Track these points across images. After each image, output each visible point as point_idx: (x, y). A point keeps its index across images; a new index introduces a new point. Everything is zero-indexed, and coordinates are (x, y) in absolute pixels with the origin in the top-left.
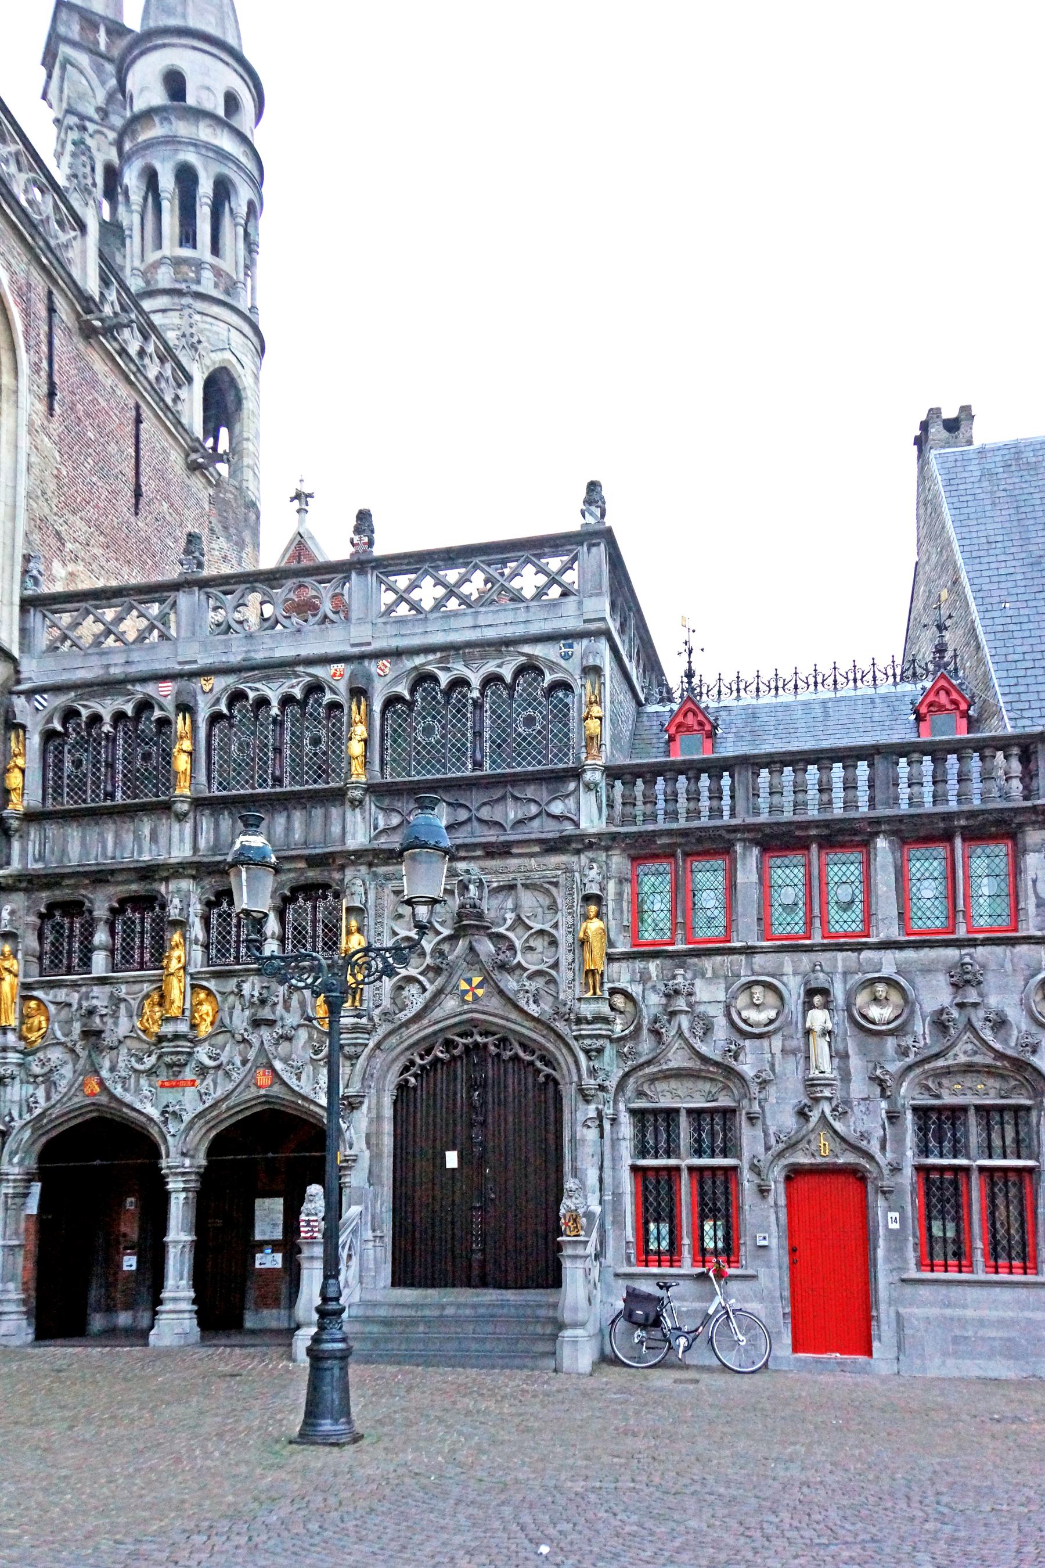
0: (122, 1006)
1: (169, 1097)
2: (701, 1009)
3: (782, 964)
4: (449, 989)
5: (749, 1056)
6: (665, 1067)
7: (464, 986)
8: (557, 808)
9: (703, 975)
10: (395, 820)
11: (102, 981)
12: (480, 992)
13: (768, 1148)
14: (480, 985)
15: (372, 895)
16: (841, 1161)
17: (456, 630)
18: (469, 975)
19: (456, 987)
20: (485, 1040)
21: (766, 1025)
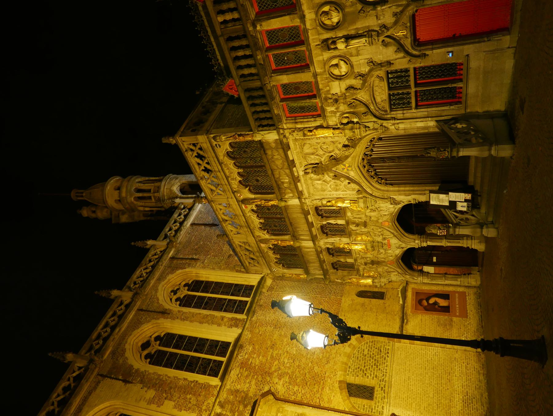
0: (363, 256)
1: (393, 246)
2: (343, 90)
3: (319, 61)
4: (347, 175)
5: (362, 70)
6: (370, 101)
7: (345, 170)
8: (273, 145)
9: (329, 91)
10: (289, 191)
11: (356, 260)
12: (347, 165)
13: (404, 57)
14: (345, 165)
15: (317, 197)
16: (408, 24)
17: (222, 177)
18: (341, 169)
19: (346, 173)
20: (365, 160)
21: (347, 64)
